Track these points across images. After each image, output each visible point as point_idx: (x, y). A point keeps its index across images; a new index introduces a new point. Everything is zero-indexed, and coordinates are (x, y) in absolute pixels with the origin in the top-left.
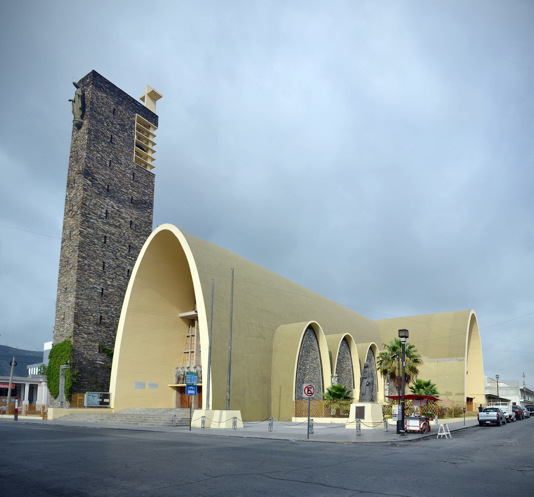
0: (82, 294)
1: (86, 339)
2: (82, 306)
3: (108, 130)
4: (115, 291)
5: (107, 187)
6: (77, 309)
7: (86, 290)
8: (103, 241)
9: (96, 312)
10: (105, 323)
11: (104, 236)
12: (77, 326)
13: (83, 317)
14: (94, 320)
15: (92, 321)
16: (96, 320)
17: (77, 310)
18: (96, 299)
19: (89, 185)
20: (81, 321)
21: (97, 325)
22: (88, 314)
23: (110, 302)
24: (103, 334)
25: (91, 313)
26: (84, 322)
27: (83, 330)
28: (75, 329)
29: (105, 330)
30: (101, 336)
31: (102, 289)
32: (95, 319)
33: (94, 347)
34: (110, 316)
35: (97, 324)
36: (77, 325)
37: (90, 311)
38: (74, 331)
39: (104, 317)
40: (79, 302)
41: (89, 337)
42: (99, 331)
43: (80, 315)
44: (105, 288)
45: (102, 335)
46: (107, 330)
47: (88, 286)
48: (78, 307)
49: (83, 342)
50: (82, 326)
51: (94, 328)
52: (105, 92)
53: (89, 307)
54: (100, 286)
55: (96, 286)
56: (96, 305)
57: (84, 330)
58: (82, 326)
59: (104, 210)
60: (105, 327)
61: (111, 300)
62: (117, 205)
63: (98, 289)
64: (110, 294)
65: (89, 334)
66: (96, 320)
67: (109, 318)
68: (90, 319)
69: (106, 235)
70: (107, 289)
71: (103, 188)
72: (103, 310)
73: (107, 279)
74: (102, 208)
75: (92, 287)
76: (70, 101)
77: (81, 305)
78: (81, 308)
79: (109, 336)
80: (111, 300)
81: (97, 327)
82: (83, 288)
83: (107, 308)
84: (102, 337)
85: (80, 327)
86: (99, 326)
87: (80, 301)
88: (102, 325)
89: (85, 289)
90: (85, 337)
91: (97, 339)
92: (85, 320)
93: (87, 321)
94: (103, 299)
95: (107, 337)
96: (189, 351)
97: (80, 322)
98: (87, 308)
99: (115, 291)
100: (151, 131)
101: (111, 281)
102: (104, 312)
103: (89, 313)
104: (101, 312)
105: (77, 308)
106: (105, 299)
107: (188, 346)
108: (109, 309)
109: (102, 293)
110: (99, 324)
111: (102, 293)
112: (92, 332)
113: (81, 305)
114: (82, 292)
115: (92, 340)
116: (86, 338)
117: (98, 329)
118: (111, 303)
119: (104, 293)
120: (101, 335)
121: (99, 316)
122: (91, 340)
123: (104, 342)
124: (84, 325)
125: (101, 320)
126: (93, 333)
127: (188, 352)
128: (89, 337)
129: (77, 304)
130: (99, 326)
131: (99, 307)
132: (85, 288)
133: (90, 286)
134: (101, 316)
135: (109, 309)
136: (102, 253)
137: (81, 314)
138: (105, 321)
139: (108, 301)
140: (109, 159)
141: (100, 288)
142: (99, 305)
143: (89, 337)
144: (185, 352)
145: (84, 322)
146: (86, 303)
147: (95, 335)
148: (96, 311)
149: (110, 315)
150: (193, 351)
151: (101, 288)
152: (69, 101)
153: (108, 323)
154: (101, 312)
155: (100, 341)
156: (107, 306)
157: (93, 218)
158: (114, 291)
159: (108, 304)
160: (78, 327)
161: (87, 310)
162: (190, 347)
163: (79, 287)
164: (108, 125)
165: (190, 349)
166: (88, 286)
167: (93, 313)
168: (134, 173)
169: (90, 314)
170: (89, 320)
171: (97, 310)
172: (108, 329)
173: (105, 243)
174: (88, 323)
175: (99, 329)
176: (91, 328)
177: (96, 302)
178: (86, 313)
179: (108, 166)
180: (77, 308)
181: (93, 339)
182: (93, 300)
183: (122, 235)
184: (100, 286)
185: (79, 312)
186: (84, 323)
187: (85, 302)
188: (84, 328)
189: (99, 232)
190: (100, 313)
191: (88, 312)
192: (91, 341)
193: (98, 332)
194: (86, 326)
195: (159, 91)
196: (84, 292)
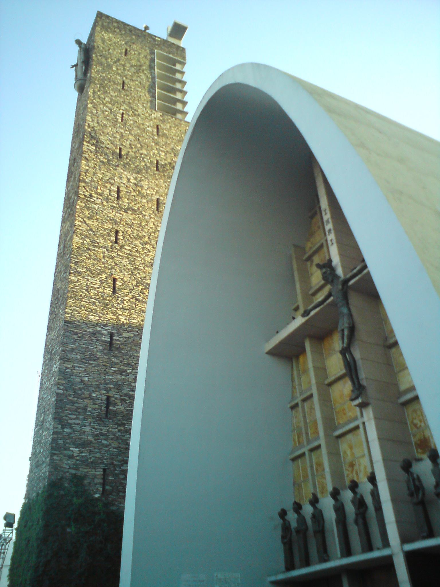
0: (72, 350)
1: (77, 460)
2: (72, 377)
3: (118, 74)
4: (135, 335)
5: (118, 151)
6: (62, 385)
7: (80, 340)
8: (113, 239)
9: (99, 388)
10: (115, 413)
11: (114, 230)
12: (60, 426)
13: (73, 403)
14: (95, 409)
15: (89, 411)
16: (98, 409)
17: (62, 387)
18: (98, 358)
19: (91, 152)
20: (69, 414)
21: (101, 420)
22: (83, 395)
23: (126, 361)
24: (111, 441)
25: (88, 390)
26: (74, 415)
27: (72, 437)
28: (56, 436)
29: (116, 430)
30: (107, 449)
31: (111, 335)
32: (96, 404)
33: (93, 480)
34: (126, 395)
35: (99, 419)
36: (59, 424)
37: (87, 386)
38: (54, 440)
39: (113, 399)
40: (67, 368)
41: (83, 454)
42: (103, 435)
43: (68, 400)
44: (115, 331)
45: (110, 445)
46: (119, 431)
47: (86, 331)
48: (65, 379)
49: (70, 468)
50: (70, 426)
51: (94, 428)
52: (114, 32)
53: (86, 379)
54: (107, 328)
55: (99, 329)
56: (98, 371)
57: (73, 435)
58: (70, 426)
59: (114, 187)
60: (117, 424)
61: (127, 357)
62: (135, 177)
63: (103, 334)
64: (124, 343)
65: (84, 445)
66: (98, 409)
67: (124, 400)
68: (86, 406)
69: (118, 229)
70: (119, 334)
71: (113, 153)
72: (111, 382)
73: (120, 313)
74: (112, 184)
75: (91, 331)
76: (72, 67)
77: (72, 374)
78: (69, 381)
79: (124, 446)
80: (127, 357)
81: (99, 425)
82: (76, 337)
83: (119, 376)
84: (109, 450)
85: (66, 430)
86: (103, 421)
87: (68, 366)
88: (110, 419)
89: (80, 337)
90: (75, 455)
91: (99, 458)
92: (76, 411)
93: (80, 414)
94: (113, 356)
95: (121, 451)
96: (305, 450)
97: (66, 416)
98: (82, 381)
99: (135, 335)
100: (178, 67)
101: (125, 316)
102: (112, 386)
103: (85, 392)
104: (109, 386)
105: (63, 382)
106: (115, 357)
107: (299, 437)
108: (123, 377)
109: (111, 343)
110: (104, 416)
111: (111, 343)
112: (90, 438)
113: (72, 374)
114: (74, 344)
115: (90, 460)
116: (77, 456)
117: (102, 430)
118: (128, 364)
119: (114, 342)
120: (107, 446)
121: (104, 397)
122: (87, 460)
123: (112, 463)
124: (75, 424)
125: (107, 407)
126: (91, 442)
127: (304, 454)
128: (83, 454)
129: (64, 373)
130: (103, 421)
131: (105, 374)
132: (80, 335)
133: (88, 330)
134: (108, 398)
135: (123, 377)
136: (110, 261)
137: (70, 395)
138: (117, 407)
139: (121, 359)
140: (121, 111)
141: (105, 332)
142: (105, 370)
143: (82, 452)
144: (293, 456)
145: (75, 417)
146: (80, 369)
147: (95, 448)
148: (98, 386)
149: (124, 392)
150: (316, 444)
151: (109, 332)
152: (71, 68)
153: (123, 412)
154: (109, 386)
155: (105, 461)
156: (121, 372)
157: (96, 202)
158: (133, 335)
159: (123, 367)
160: (61, 430)
161: (81, 386)
162: (304, 435)
163: (68, 334)
164: (117, 69)
165: (305, 443)
166: (86, 331)
167: (93, 391)
168: (157, 126)
169: (87, 393)
170: (85, 409)
171: (101, 384)
172: (122, 428)
173: (116, 242)
174: (82, 417)
175: (105, 430)
176: (87, 429)
177: (98, 365)
178: (80, 392)
179: (120, 121)
180: (63, 382)
181: (91, 458)
182: (94, 360)
183: (143, 224)
184: (107, 328)
185: (65, 392)
186: (74, 419)
187: (78, 367)
188: (74, 431)
189: (106, 225)
190: (106, 389)
191: (83, 391)
192: (86, 466)
193: (101, 437)
194: (78, 424)
195: (182, 22)
196: (77, 344)
